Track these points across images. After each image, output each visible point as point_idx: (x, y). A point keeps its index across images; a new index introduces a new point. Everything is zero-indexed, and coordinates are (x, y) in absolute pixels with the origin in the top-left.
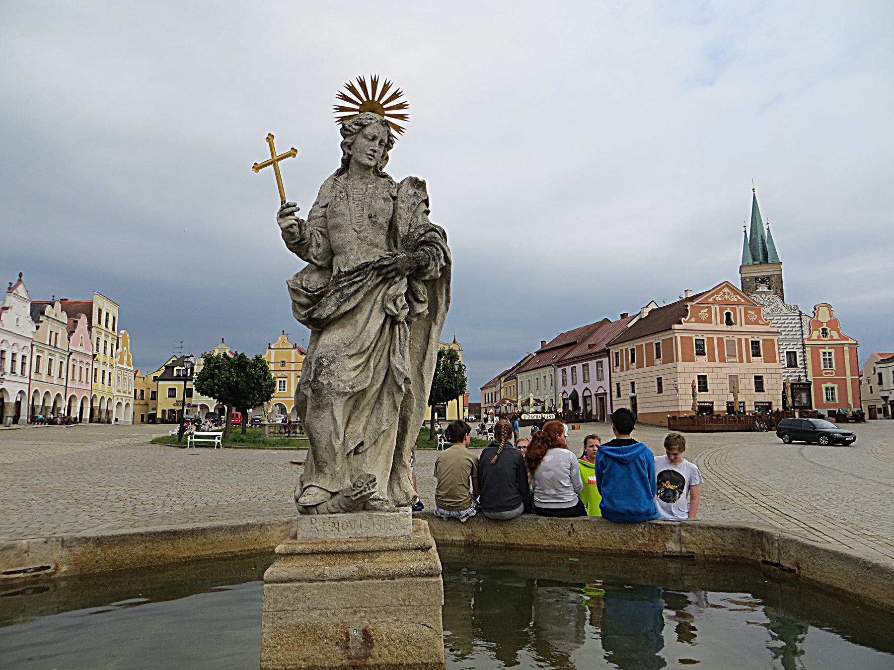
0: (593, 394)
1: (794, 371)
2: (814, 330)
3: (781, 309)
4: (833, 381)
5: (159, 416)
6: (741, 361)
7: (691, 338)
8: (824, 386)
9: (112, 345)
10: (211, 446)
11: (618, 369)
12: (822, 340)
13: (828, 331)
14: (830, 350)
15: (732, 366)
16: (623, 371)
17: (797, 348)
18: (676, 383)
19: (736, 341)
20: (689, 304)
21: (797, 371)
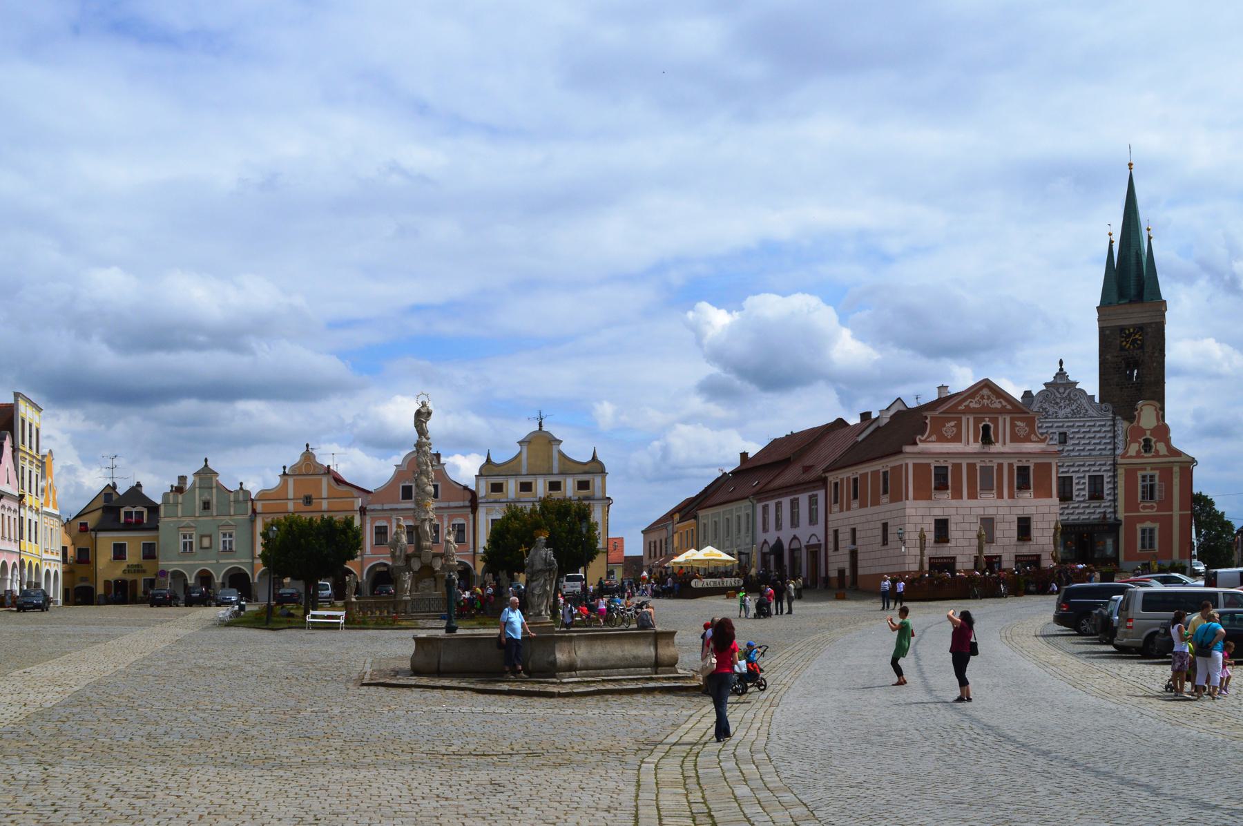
0: (803, 546)
2: (1131, 442)
3: (1087, 411)
5: (100, 590)
6: (1000, 496)
7: (929, 465)
9: (37, 475)
10: (334, 627)
11: (836, 508)
12: (1143, 457)
13: (1153, 443)
14: (1152, 472)
15: (987, 504)
16: (843, 511)
17: (1105, 471)
18: (900, 531)
19: (995, 468)
20: (929, 414)
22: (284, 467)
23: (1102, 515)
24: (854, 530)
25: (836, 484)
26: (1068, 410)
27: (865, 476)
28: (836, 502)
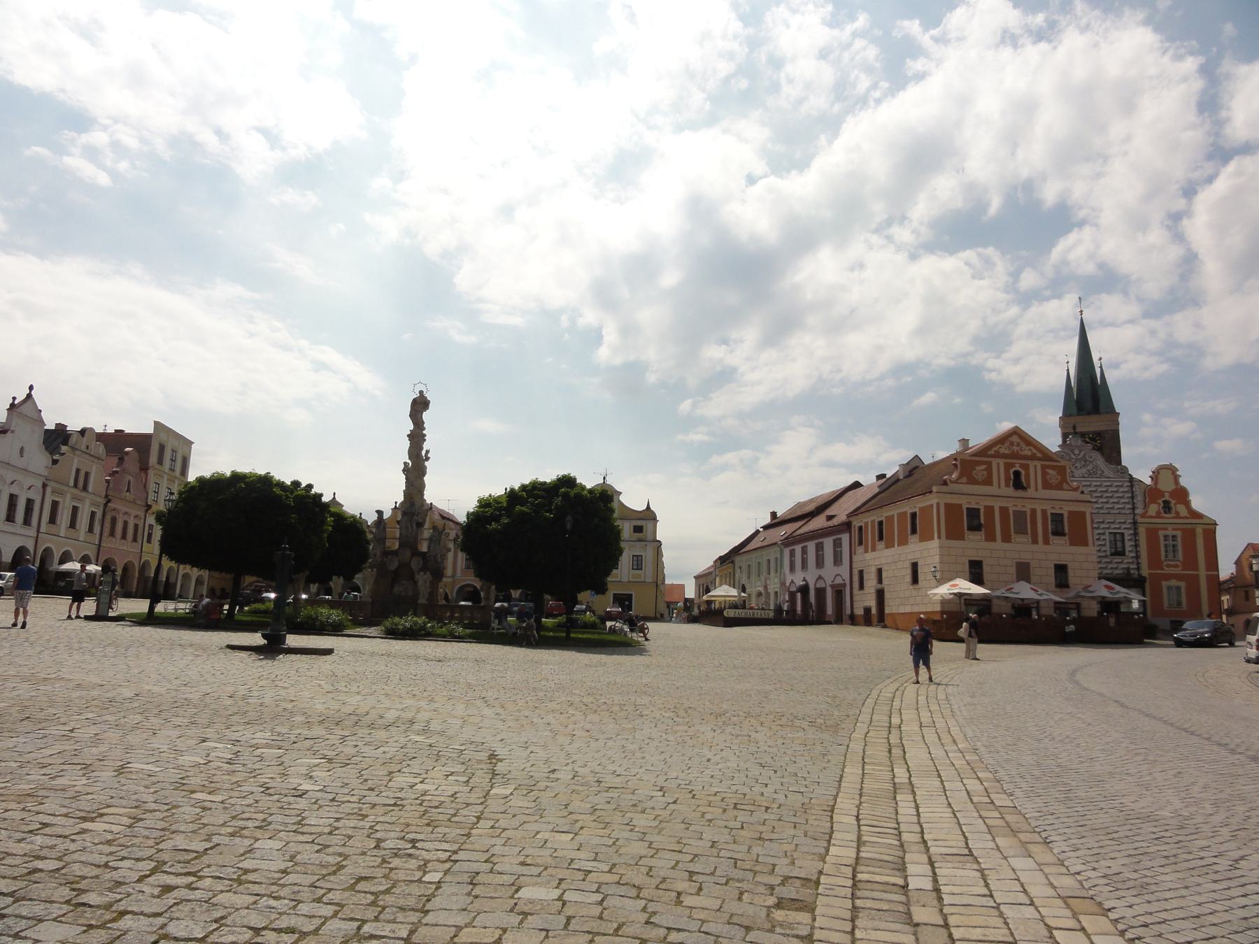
0: (828, 585)
1: (1120, 560)
4: (1179, 577)
6: (1035, 541)
7: (960, 506)
8: (1165, 584)
11: (860, 550)
12: (1163, 517)
13: (1172, 505)
14: (1174, 533)
15: (1021, 548)
17: (1125, 528)
19: (1029, 513)
21: (1125, 561)
22: (396, 503)
23: (1125, 571)
24: (880, 571)
25: (860, 528)
26: (1084, 470)
27: (890, 518)
28: (861, 543)
